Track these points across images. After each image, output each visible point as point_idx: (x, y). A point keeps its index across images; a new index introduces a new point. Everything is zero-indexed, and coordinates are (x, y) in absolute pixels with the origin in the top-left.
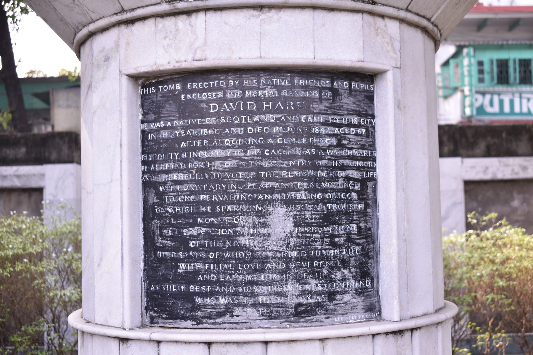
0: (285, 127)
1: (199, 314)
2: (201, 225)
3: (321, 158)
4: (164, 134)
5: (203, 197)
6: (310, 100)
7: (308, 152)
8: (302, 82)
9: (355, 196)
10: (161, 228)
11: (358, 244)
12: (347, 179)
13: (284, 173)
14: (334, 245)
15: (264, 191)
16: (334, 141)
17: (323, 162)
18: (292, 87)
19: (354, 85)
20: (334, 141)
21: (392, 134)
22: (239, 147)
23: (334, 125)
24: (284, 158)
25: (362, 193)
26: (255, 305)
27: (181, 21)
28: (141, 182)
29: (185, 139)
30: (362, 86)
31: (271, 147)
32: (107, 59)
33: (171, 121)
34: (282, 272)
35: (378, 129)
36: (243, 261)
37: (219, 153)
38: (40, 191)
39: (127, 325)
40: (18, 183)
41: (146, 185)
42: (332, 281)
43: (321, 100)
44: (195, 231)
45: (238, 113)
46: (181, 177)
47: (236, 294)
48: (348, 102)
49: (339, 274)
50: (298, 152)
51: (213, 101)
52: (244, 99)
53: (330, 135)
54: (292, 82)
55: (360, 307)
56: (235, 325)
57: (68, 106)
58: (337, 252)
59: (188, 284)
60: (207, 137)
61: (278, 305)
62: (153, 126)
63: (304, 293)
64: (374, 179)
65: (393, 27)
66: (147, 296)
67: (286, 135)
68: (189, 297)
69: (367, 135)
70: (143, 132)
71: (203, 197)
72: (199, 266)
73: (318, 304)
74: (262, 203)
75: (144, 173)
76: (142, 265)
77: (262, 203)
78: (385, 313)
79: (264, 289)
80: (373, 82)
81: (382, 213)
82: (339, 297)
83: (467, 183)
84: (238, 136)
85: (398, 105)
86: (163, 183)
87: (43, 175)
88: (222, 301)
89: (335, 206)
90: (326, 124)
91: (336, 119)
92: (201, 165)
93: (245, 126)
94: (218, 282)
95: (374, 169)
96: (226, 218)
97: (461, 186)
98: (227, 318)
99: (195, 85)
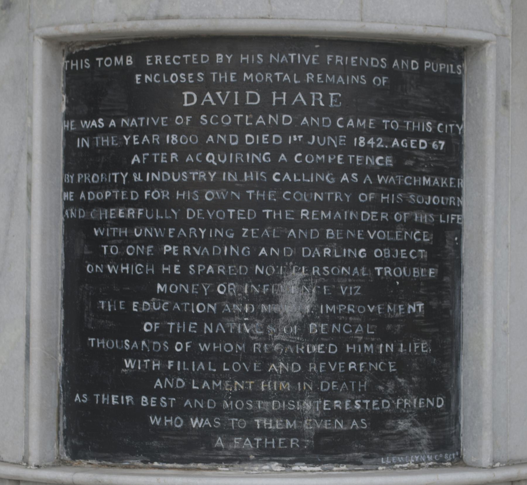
4: (105, 141)
5: (167, 248)
7: (345, 178)
8: (339, 59)
11: (425, 337)
12: (411, 225)
13: (304, 213)
14: (387, 337)
15: (268, 243)
16: (389, 161)
19: (428, 65)
20: (389, 161)
23: (390, 134)
28: (62, 219)
29: (139, 150)
30: (441, 66)
31: (283, 168)
33: (118, 119)
34: (294, 379)
35: (468, 142)
36: (230, 358)
39: (34, 460)
45: (230, 109)
47: (219, 411)
49: (391, 386)
50: (327, 178)
55: (424, 442)
58: (390, 347)
60: (177, 148)
61: (288, 433)
62: (85, 124)
64: (457, 228)
66: (66, 413)
70: (67, 134)
71: (167, 248)
72: (156, 365)
73: (354, 434)
74: (264, 261)
75: (67, 204)
76: (60, 359)
77: (264, 261)
78: (467, 453)
80: (461, 60)
82: (390, 423)
86: (102, 224)
88: (195, 423)
89: (388, 271)
91: (395, 124)
92: (165, 195)
94: (188, 392)
95: (458, 210)
99: (158, 59)
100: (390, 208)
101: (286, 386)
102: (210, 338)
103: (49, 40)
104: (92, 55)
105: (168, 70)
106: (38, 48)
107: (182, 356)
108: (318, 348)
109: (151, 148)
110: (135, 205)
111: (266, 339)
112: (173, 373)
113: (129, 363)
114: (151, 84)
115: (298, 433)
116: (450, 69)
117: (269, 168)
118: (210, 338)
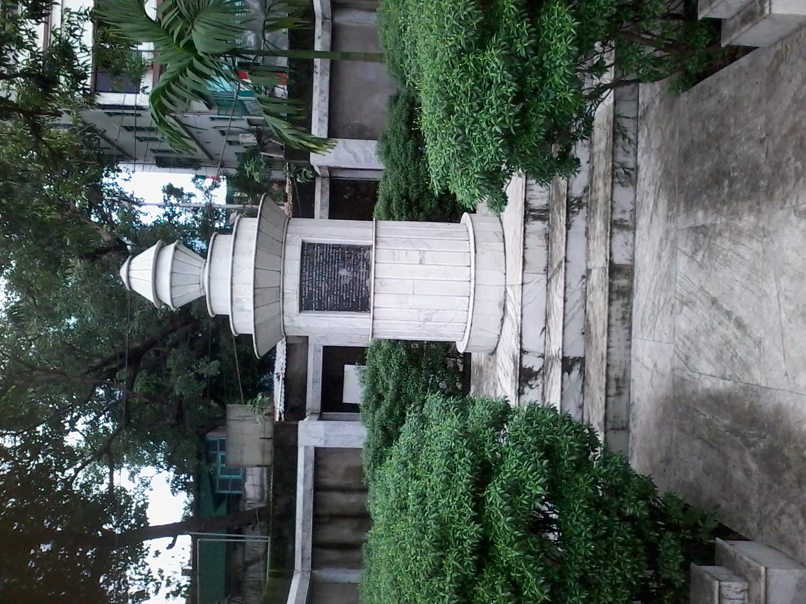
18: (306, 267)
25: (338, 249)
27: (286, 297)
38: (317, 450)
40: (311, 466)
41: (330, 310)
48: (310, 251)
56: (370, 287)
57: (242, 453)
65: (288, 236)
81: (343, 243)
85: (311, 236)
87: (306, 447)
103: (301, 310)
106: (301, 314)
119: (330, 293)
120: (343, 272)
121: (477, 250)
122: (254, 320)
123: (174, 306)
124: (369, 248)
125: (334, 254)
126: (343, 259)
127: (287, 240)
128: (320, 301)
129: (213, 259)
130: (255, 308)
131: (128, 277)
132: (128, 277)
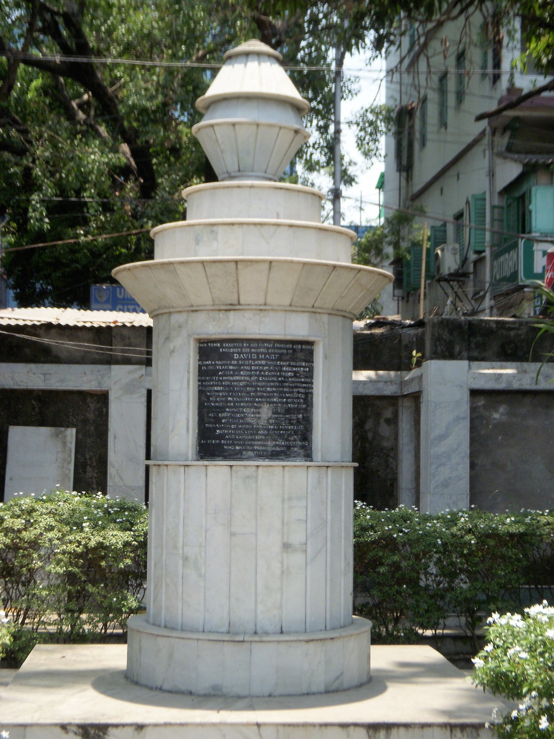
0: (269, 367)
1: (226, 454)
2: (228, 412)
3: (286, 382)
4: (211, 367)
5: (229, 399)
6: (282, 354)
8: (278, 345)
9: (302, 401)
10: (208, 413)
11: (302, 424)
12: (298, 392)
13: (268, 389)
14: (291, 424)
15: (258, 397)
17: (287, 384)
18: (274, 348)
19: (304, 346)
20: (293, 374)
21: (321, 372)
22: (247, 376)
23: (293, 366)
24: (269, 381)
25: (305, 399)
26: (253, 450)
27: (222, 315)
29: (221, 370)
31: (262, 376)
32: (180, 327)
36: (248, 430)
37: (238, 378)
42: (289, 441)
43: (287, 353)
44: (225, 415)
45: (248, 359)
46: (219, 388)
47: (244, 445)
48: (300, 355)
49: (292, 438)
50: (275, 379)
51: (236, 353)
52: (251, 353)
53: (291, 372)
54: (274, 345)
58: (292, 427)
59: (220, 440)
60: (233, 370)
61: (263, 451)
63: (275, 446)
64: (312, 393)
67: (270, 371)
68: (222, 445)
69: (309, 371)
70: (199, 365)
71: (229, 399)
73: (282, 452)
74: (257, 402)
75: (199, 386)
77: (257, 402)
79: (256, 443)
82: (292, 448)
83: (474, 393)
84: (247, 370)
85: (326, 357)
86: (210, 391)
88: (237, 448)
89: (292, 405)
90: (289, 366)
92: (228, 383)
93: (251, 365)
94: (235, 439)
95: (312, 388)
96: (240, 409)
97: (466, 396)
98: (239, 456)
99: (227, 345)
100: (292, 387)
101: (263, 437)
102: (242, 424)
104: (207, 343)
105: (230, 348)
107: (234, 429)
108: (272, 427)
109: (225, 370)
110: (220, 386)
111: (258, 424)
112: (231, 434)
113: (218, 431)
114: (225, 352)
115: (266, 451)
116: (310, 347)
117: (259, 376)
118: (242, 424)
119: (230, 389)
120: (266, 412)
121: (311, 644)
122: (182, 263)
123: (199, 129)
124: (308, 456)
125: (296, 395)
126: (288, 411)
127: (318, 316)
128: (215, 373)
129: (282, 192)
130: (203, 262)
131: (247, 55)
132: (247, 55)
